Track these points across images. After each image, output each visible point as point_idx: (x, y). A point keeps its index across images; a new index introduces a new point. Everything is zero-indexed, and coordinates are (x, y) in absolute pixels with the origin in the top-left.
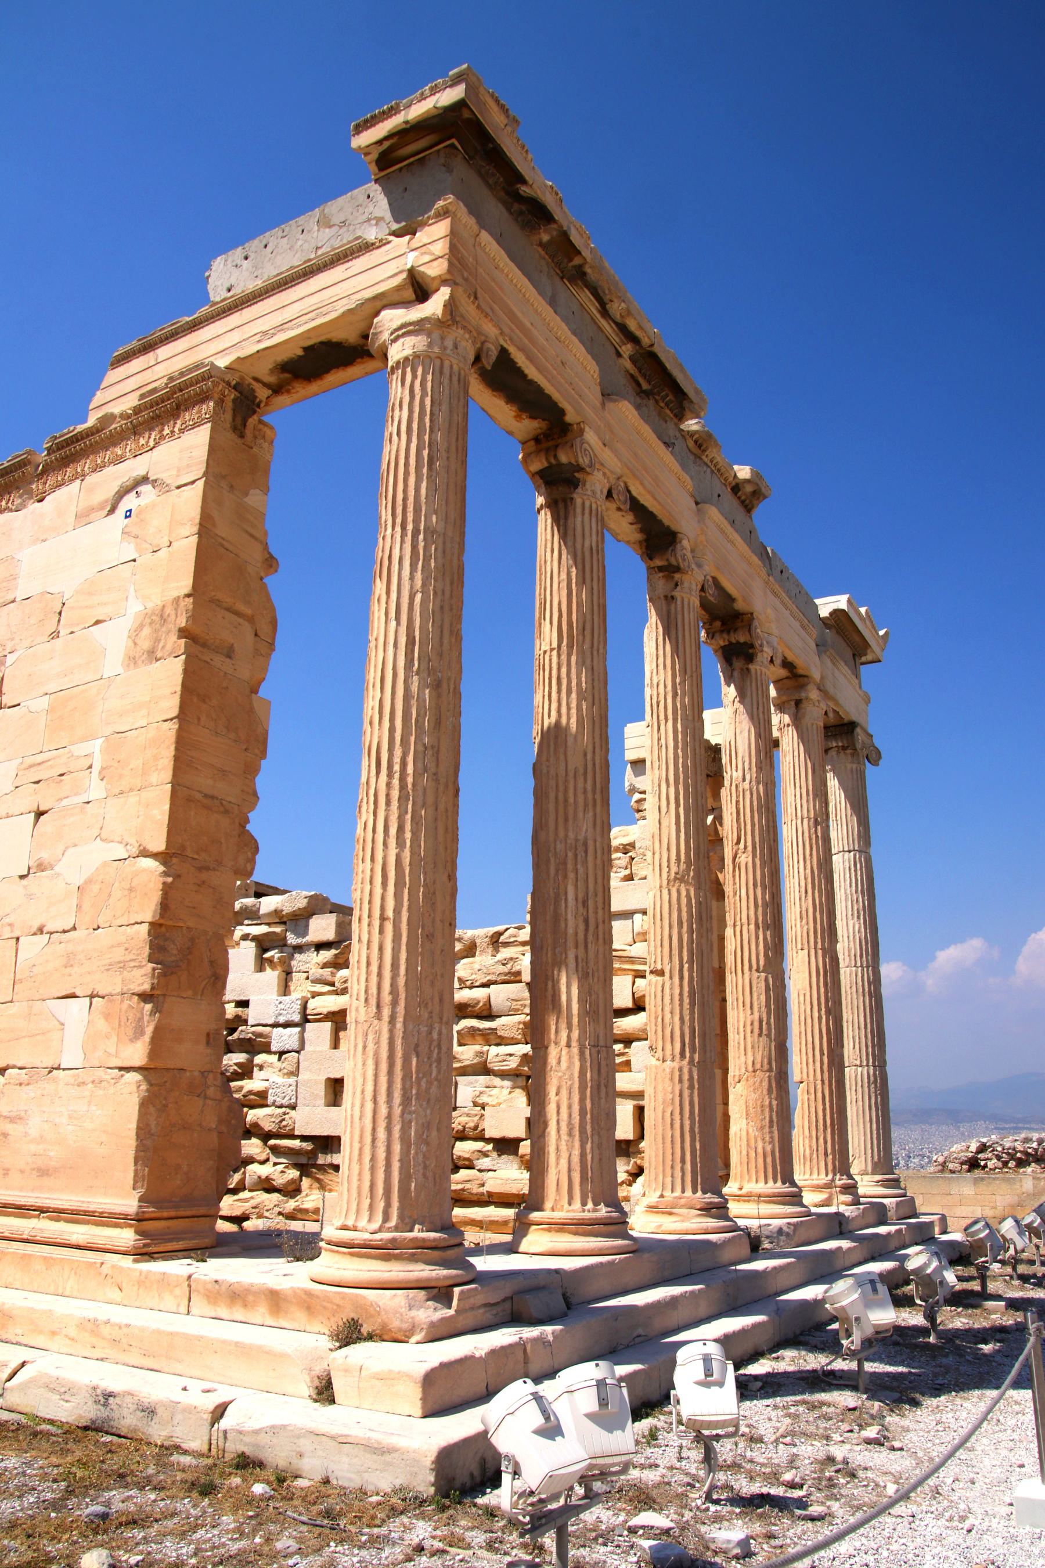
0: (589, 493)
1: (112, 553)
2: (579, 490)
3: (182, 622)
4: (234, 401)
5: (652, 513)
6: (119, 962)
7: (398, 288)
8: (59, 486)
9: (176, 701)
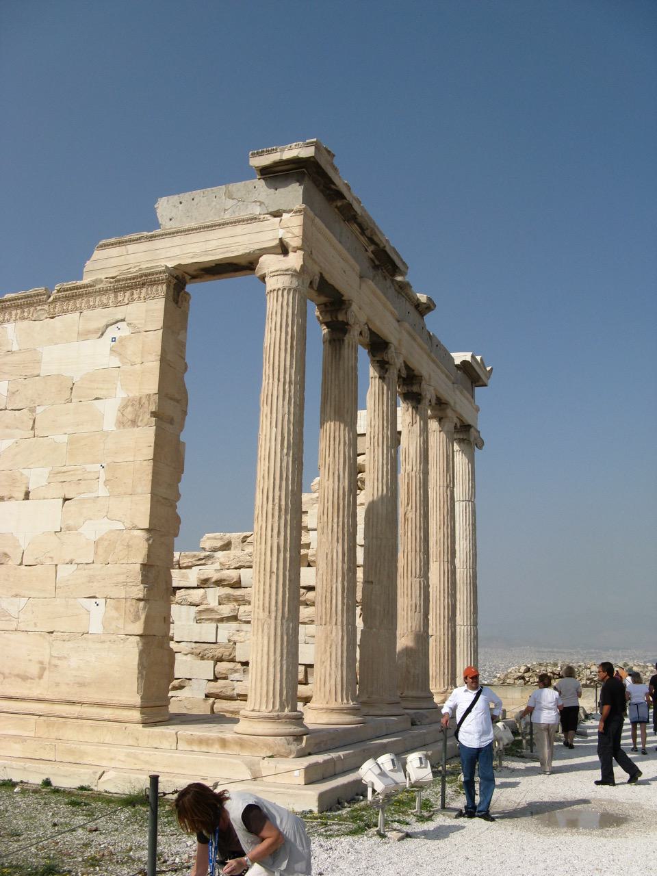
0: (352, 337)
1: (101, 355)
2: (347, 335)
3: (153, 408)
4: (175, 284)
5: (378, 335)
6: (123, 582)
7: (273, 247)
8: (64, 312)
9: (151, 450)
